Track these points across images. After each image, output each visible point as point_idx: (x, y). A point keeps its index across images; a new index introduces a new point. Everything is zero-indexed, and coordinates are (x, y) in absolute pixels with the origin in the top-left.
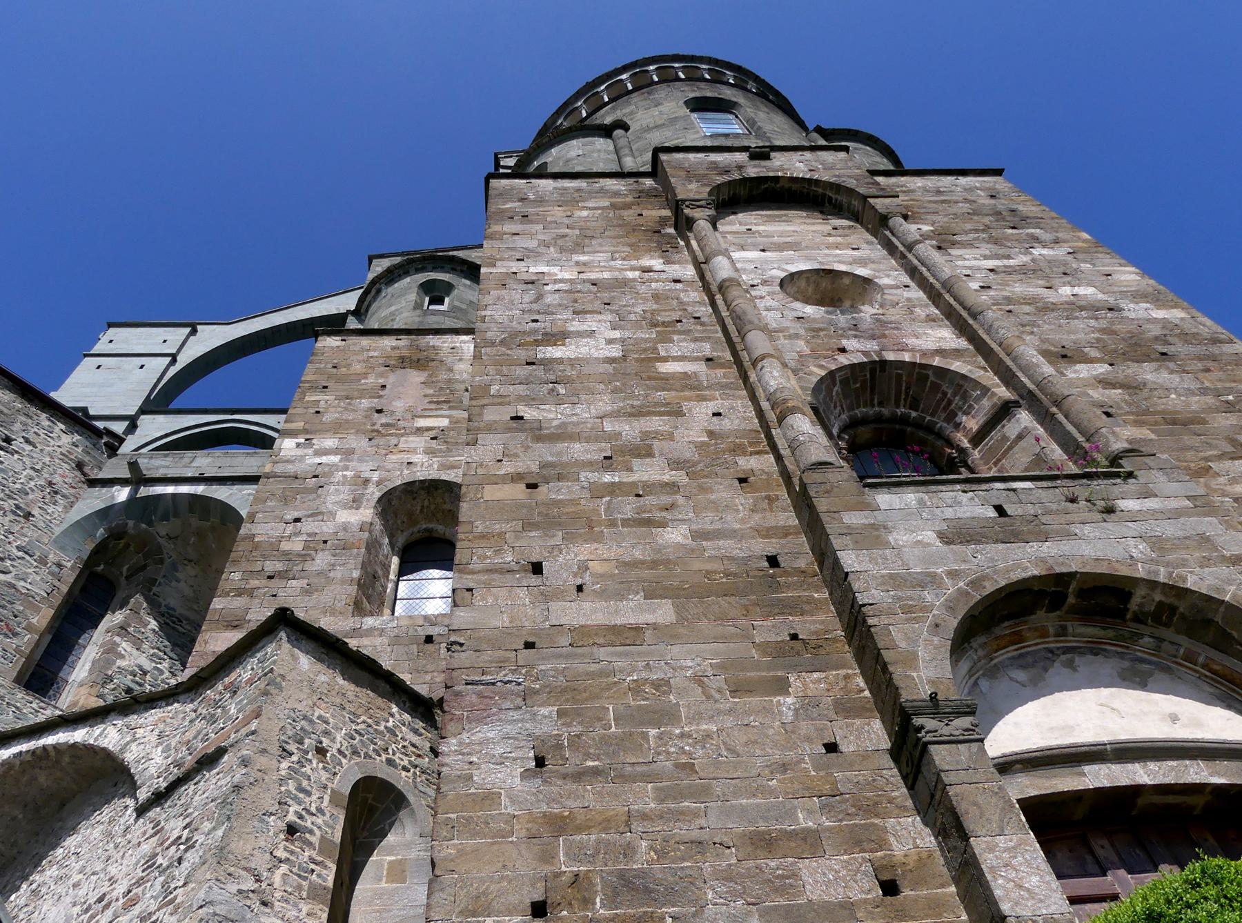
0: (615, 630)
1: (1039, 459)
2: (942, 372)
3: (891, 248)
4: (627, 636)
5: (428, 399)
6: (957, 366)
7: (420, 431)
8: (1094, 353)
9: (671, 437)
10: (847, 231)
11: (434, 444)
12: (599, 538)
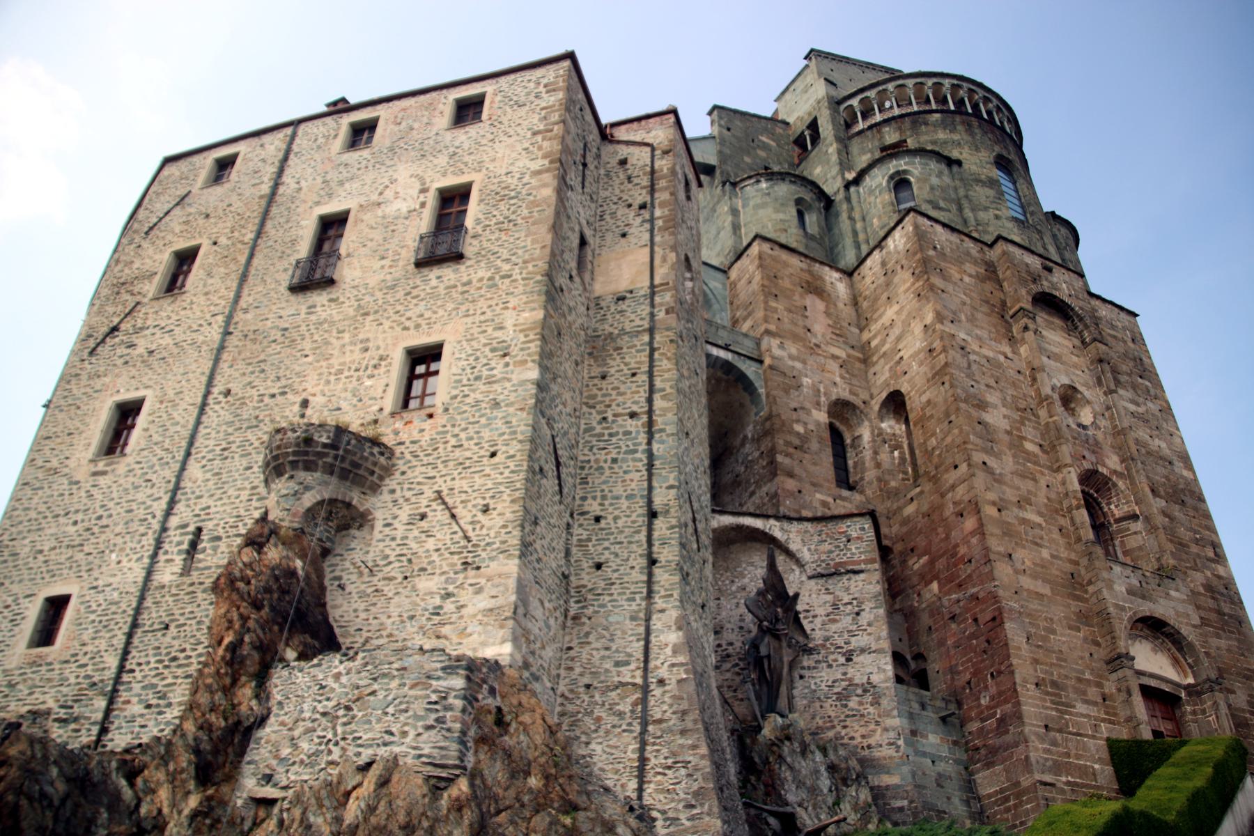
0: (1037, 593)
1: (1140, 548)
2: (1115, 485)
4: (1040, 596)
5: (830, 330)
6: (1121, 484)
7: (834, 357)
8: (1162, 493)
9: (1036, 496)
11: (843, 371)
12: (1024, 547)
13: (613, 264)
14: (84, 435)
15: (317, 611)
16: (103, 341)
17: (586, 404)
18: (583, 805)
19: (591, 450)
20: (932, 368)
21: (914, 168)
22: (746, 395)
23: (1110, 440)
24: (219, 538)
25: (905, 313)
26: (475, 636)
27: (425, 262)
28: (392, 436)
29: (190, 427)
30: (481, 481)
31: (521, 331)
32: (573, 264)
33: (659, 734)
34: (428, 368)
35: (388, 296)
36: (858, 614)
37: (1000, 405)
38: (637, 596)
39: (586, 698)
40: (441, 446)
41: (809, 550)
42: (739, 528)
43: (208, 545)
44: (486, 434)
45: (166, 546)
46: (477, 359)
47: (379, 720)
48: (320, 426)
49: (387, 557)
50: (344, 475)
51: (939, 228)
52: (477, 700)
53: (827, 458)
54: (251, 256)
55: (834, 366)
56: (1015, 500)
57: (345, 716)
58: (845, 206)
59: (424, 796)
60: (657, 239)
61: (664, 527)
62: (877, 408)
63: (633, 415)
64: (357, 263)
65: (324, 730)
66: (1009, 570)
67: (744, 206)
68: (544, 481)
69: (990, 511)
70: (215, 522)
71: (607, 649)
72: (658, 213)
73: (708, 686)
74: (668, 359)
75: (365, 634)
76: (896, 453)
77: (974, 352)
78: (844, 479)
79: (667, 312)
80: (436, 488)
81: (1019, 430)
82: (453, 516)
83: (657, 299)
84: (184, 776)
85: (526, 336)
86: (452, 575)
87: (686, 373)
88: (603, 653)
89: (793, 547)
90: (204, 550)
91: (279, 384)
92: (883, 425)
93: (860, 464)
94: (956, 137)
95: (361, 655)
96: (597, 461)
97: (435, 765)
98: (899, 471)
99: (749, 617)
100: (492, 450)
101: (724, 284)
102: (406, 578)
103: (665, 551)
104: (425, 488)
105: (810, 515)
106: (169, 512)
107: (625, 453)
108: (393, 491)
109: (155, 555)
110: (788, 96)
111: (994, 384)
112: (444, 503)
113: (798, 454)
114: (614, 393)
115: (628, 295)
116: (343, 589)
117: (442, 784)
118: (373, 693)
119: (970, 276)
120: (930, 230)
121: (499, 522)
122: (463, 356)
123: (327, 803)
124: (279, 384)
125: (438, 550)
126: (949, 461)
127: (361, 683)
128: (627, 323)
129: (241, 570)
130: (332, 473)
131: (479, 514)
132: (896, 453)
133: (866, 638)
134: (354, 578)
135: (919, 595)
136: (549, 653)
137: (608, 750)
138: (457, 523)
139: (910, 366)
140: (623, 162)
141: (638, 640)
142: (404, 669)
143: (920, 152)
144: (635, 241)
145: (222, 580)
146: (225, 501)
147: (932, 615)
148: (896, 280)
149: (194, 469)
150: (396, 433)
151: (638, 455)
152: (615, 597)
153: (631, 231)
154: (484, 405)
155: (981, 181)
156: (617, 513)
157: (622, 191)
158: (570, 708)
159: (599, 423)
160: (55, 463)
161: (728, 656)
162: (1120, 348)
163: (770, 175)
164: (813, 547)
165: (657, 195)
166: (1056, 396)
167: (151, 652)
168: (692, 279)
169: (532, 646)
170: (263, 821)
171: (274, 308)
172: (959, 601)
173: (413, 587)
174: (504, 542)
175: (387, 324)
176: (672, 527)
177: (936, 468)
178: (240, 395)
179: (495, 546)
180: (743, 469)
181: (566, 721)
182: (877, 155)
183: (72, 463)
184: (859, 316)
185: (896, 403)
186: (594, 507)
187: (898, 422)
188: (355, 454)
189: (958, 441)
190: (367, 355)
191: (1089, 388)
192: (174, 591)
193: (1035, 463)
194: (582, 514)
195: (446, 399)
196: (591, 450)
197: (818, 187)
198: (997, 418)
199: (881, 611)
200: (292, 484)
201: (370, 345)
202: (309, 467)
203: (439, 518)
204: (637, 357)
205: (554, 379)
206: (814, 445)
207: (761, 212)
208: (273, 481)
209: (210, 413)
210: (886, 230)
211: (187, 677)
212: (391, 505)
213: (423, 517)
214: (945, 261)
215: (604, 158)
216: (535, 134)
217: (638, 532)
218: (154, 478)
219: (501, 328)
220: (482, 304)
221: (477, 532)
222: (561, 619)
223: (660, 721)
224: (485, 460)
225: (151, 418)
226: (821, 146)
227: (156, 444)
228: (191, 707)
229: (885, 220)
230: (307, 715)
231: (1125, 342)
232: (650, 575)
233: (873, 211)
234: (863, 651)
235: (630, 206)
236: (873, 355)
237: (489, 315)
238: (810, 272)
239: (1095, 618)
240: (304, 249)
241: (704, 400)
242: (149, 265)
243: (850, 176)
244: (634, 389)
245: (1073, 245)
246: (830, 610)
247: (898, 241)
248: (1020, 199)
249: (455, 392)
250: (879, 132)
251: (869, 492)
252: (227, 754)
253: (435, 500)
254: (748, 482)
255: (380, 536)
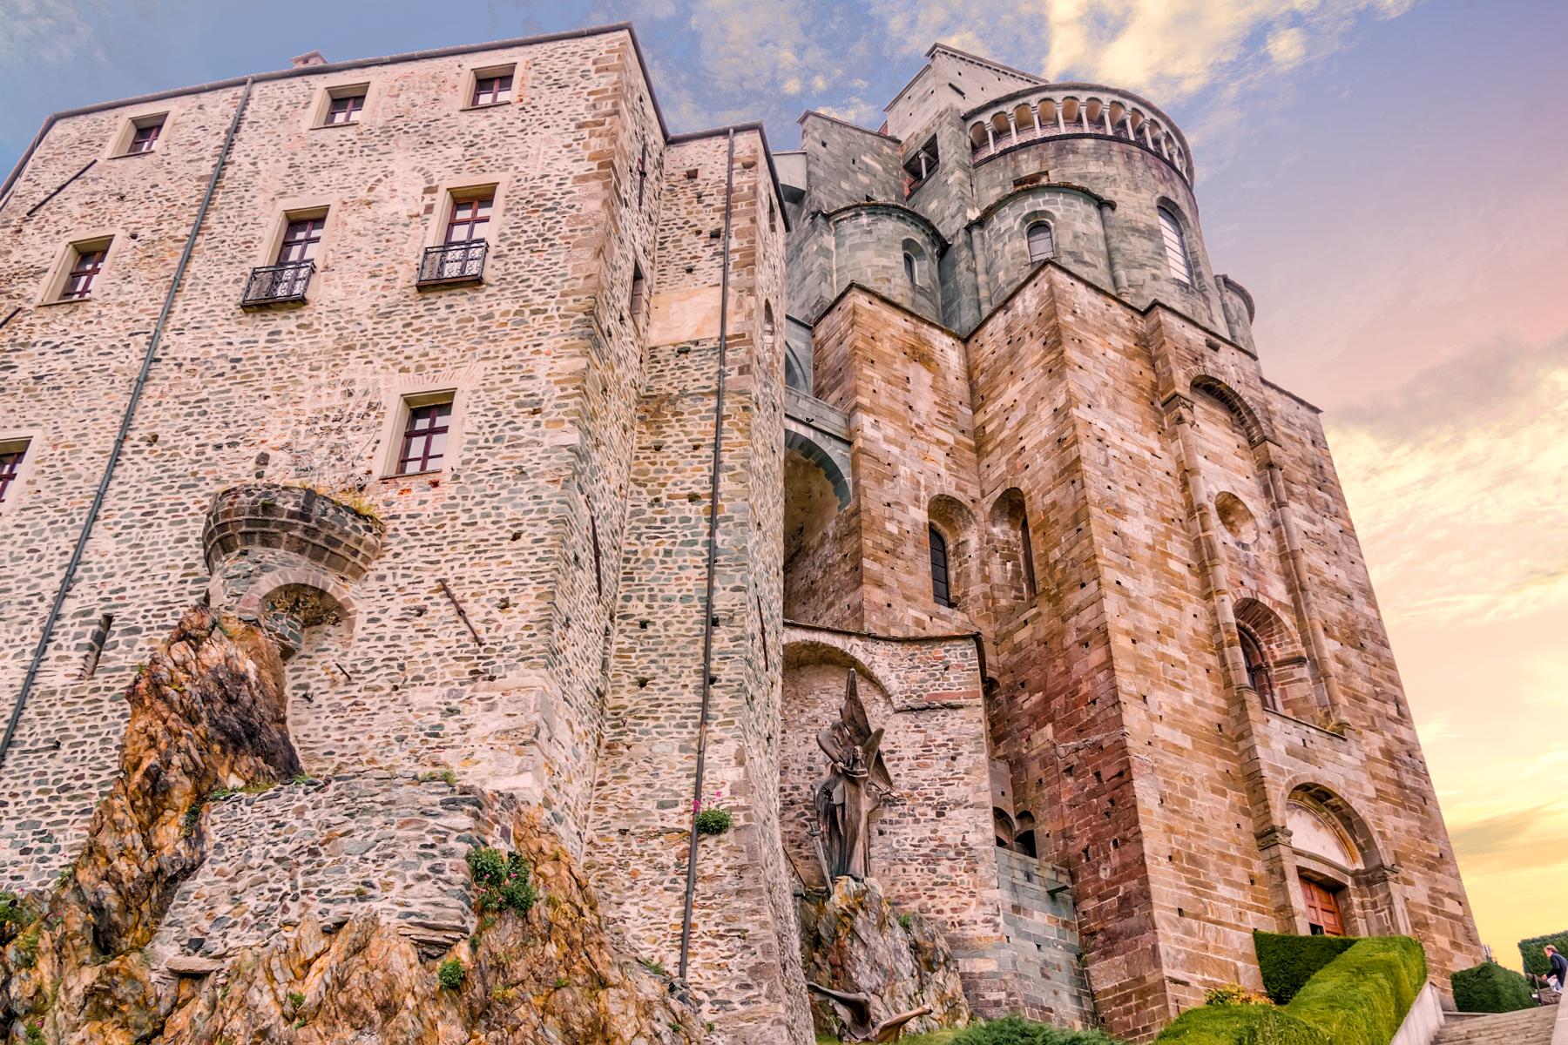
3: (1267, 492)
6: (1287, 619)
7: (940, 443)
10: (1244, 454)
12: (1161, 688)
13: (674, 308)
15: (273, 728)
17: (634, 480)
18: (614, 981)
19: (638, 539)
20: (1061, 462)
21: (1056, 206)
22: (829, 483)
23: (1275, 563)
24: (137, 631)
25: (1031, 393)
26: (484, 764)
27: (429, 286)
28: (382, 507)
29: (97, 482)
30: (501, 569)
31: (556, 382)
32: (625, 302)
33: (710, 894)
34: (433, 422)
35: (380, 326)
36: (953, 759)
37: (1142, 512)
38: (690, 722)
39: (621, 847)
40: (449, 523)
41: (898, 677)
42: (814, 646)
43: (121, 640)
44: (508, 511)
45: (59, 639)
46: (498, 415)
47: (355, 869)
48: (285, 488)
49: (371, 660)
50: (317, 554)
51: (1080, 287)
52: (486, 844)
53: (924, 566)
55: (938, 454)
56: (1155, 630)
57: (307, 862)
58: (964, 253)
59: (411, 966)
60: (732, 278)
61: (726, 638)
62: (988, 508)
63: (693, 498)
64: (343, 281)
65: (279, 880)
66: (1143, 716)
67: (837, 246)
68: (579, 574)
69: (1121, 642)
70: (132, 609)
71: (649, 786)
72: (734, 244)
73: (771, 838)
74: (740, 430)
75: (338, 760)
76: (1009, 565)
77: (1115, 447)
78: (944, 594)
79: (741, 372)
80: (440, 575)
81: (1163, 544)
82: (461, 612)
83: (729, 355)
84: (77, 942)
85: (562, 390)
86: (456, 686)
87: (761, 451)
88: (644, 790)
89: (878, 672)
90: (115, 645)
91: (227, 432)
92: (995, 530)
93: (964, 576)
94: (1111, 171)
95: (334, 784)
96: (645, 552)
97: (427, 927)
98: (1012, 588)
99: (820, 756)
100: (515, 530)
101: (808, 344)
102: (396, 688)
103: (727, 668)
104: (425, 575)
105: (900, 635)
106: (63, 594)
107: (682, 544)
108: (382, 578)
109: (40, 652)
110: (901, 105)
111: (1135, 486)
112: (449, 595)
113: (889, 559)
114: (670, 469)
115: (693, 347)
116: (310, 700)
117: (435, 952)
118: (349, 833)
119: (1116, 350)
120: (1070, 289)
122: (481, 410)
123: (278, 975)
124: (227, 432)
125: (438, 654)
126: (1075, 577)
127: (333, 820)
128: (690, 383)
129: (171, 672)
130: (301, 551)
131: (496, 610)
132: (1009, 565)
133: (962, 788)
134: (325, 686)
135: (1028, 740)
136: (577, 788)
137: (645, 913)
138: (466, 622)
139: (1033, 459)
140: (692, 175)
141: (688, 776)
142: (391, 802)
143: (1065, 188)
144: (703, 278)
145: (143, 684)
146: (147, 581)
147: (1044, 765)
148: (1022, 351)
149: (102, 540)
150: (389, 504)
151: (698, 548)
152: (662, 722)
153: (699, 265)
154: (505, 474)
155: (1138, 230)
156: (668, 618)
157: (690, 213)
158: (600, 858)
159: (651, 505)
161: (792, 803)
162: (1296, 451)
163: (873, 208)
164: (902, 674)
165: (733, 221)
166: (1212, 506)
167: (32, 779)
168: (772, 333)
169: (556, 778)
170: (186, 1001)
171: (220, 331)
172: (1077, 750)
173: (405, 699)
174: (523, 647)
175: (378, 362)
176: (736, 639)
177: (1058, 586)
178: (171, 443)
179: (514, 652)
180: (820, 575)
181: (594, 875)
182: (1010, 190)
184: (973, 392)
185: (1012, 505)
186: (639, 609)
187: (1013, 527)
188: (333, 528)
189: (1087, 553)
190: (352, 401)
191: (1253, 498)
192: (68, 698)
193: (1182, 587)
194: (623, 617)
195: (457, 464)
196: (638, 539)
197: (933, 228)
198: (1138, 529)
199: (983, 757)
200: (244, 561)
201: (357, 388)
202: (267, 541)
203: (443, 613)
204: (702, 428)
205: (597, 446)
206: (910, 550)
207: (859, 255)
208: (218, 558)
209: (127, 464)
210: (1014, 286)
211: (83, 812)
212: (378, 595)
213: (421, 612)
214: (1086, 330)
215: (668, 168)
217: (695, 642)
218: (43, 547)
219: (531, 377)
220: (507, 345)
221: (492, 633)
222: (593, 746)
223: (712, 878)
224: (505, 542)
225: (39, 467)
226: (939, 175)
227: (46, 502)
228: (91, 851)
229: (1014, 274)
230: (255, 862)
231: (1303, 444)
232: (706, 696)
233: (999, 262)
234: (957, 804)
235: (699, 233)
236: (988, 442)
237: (515, 359)
238: (917, 335)
239: (1252, 782)
240: (264, 256)
241: (781, 485)
243: (973, 215)
244: (696, 465)
245: (1247, 318)
246: (920, 751)
247: (1028, 302)
248: (1185, 256)
249: (468, 455)
250: (1014, 159)
251: (972, 610)
252: (141, 913)
253: (437, 591)
254: (826, 590)
255: (363, 635)
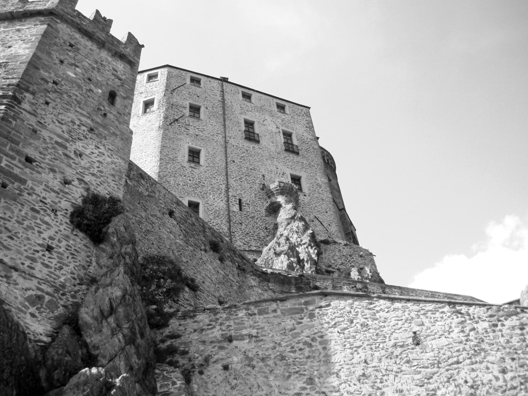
14: (180, 152)
16: (174, 122)
54: (224, 120)
82: (322, 224)
121: (334, 230)
149: (231, 181)
160: (171, 156)
183: (180, 159)
202: (291, 196)
213: (313, 221)
216: (307, 127)
237: (311, 175)
242: (180, 103)
